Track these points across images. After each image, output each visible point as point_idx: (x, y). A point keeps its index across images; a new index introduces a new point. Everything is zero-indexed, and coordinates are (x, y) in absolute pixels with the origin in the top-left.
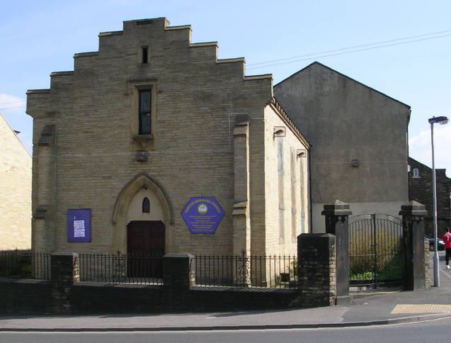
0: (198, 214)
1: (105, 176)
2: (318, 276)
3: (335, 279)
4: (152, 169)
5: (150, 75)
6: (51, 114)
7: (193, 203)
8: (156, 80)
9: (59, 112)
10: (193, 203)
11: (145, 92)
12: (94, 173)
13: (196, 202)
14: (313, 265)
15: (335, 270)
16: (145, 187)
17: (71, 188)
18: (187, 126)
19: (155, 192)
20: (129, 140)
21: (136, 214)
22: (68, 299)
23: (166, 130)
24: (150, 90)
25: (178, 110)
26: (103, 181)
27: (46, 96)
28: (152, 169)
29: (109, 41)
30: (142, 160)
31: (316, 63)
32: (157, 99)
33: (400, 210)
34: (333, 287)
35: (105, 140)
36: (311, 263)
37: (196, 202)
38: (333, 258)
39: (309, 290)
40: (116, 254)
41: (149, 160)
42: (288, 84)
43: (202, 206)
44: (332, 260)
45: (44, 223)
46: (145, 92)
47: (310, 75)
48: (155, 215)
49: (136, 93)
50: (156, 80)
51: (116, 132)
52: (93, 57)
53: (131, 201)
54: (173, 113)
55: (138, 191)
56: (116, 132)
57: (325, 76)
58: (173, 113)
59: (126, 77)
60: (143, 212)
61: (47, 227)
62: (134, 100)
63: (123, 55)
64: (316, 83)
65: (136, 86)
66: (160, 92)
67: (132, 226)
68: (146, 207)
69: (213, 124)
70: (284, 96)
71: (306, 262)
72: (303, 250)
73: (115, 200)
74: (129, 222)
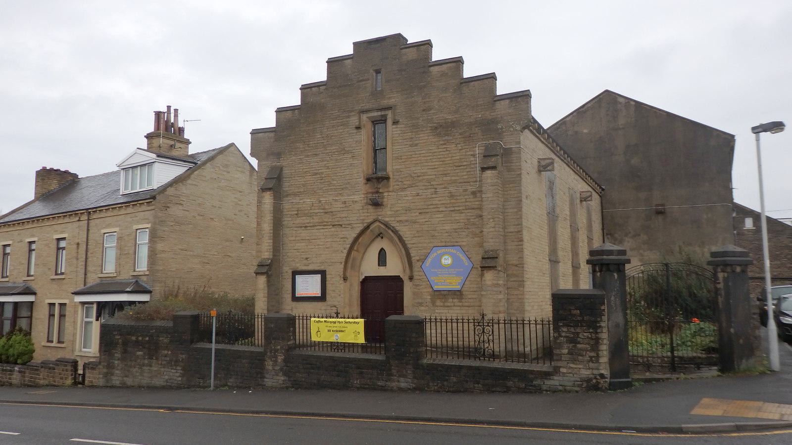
0: (442, 266)
2: (582, 349)
7: (435, 254)
8: (389, 108)
10: (435, 254)
13: (439, 252)
16: (380, 235)
19: (391, 240)
20: (362, 180)
21: (370, 267)
26: (333, 229)
28: (386, 214)
30: (376, 204)
36: (572, 330)
37: (439, 252)
41: (384, 203)
43: (446, 257)
44: (600, 327)
49: (369, 126)
50: (389, 108)
53: (364, 253)
55: (373, 241)
60: (379, 265)
61: (269, 284)
67: (367, 282)
70: (570, 133)
72: (561, 312)
74: (363, 277)
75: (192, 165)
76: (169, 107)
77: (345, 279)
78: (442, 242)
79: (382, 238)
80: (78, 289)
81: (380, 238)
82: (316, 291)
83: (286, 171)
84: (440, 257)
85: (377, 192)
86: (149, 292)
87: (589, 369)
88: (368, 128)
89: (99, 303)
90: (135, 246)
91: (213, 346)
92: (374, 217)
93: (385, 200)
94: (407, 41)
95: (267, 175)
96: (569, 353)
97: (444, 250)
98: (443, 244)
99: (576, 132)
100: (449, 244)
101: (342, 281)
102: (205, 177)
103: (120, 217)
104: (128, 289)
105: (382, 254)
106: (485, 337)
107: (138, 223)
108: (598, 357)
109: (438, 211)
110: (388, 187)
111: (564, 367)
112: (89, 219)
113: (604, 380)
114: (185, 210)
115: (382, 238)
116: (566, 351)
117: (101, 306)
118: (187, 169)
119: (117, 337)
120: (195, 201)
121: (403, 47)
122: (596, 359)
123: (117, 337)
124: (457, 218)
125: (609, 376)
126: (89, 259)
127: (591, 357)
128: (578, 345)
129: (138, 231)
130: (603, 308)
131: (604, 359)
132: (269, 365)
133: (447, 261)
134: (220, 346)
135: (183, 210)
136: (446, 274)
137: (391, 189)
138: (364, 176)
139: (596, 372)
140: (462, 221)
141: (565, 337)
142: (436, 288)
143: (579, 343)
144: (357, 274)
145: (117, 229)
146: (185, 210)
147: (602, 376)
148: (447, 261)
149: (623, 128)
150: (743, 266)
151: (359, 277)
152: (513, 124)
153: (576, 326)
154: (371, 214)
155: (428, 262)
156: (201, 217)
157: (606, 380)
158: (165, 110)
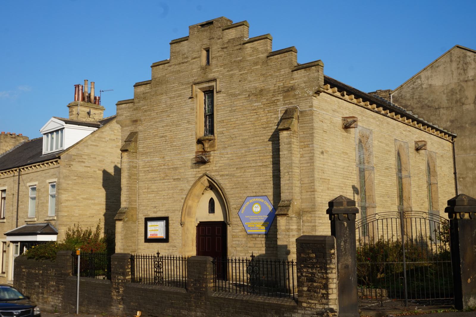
0: (253, 214)
1: (176, 178)
2: (317, 287)
3: (335, 291)
5: (211, 76)
6: (135, 121)
7: (248, 203)
8: (215, 80)
9: (140, 120)
10: (248, 203)
13: (251, 201)
15: (335, 281)
22: (122, 299)
26: (174, 183)
29: (177, 47)
32: (217, 98)
33: (446, 206)
36: (310, 270)
37: (251, 201)
38: (332, 266)
39: (309, 303)
40: (156, 255)
41: (211, 160)
43: (256, 205)
44: (330, 268)
48: (218, 216)
50: (215, 80)
52: (166, 65)
54: (230, 111)
57: (468, 59)
58: (230, 111)
59: (191, 80)
60: (209, 213)
63: (189, 59)
64: (458, 68)
65: (200, 89)
68: (212, 209)
69: (265, 120)
70: (424, 86)
71: (305, 270)
72: (302, 255)
73: (183, 201)
74: (199, 222)
75: (95, 129)
78: (253, 192)
80: (9, 231)
82: (161, 234)
84: (252, 205)
86: (56, 233)
87: (322, 304)
88: (201, 96)
89: (21, 242)
92: (204, 172)
95: (127, 138)
96: (308, 290)
97: (254, 199)
98: (254, 194)
100: (258, 194)
101: (180, 226)
102: (105, 138)
103: (39, 173)
105: (212, 202)
106: (254, 276)
107: (50, 177)
108: (328, 294)
109: (250, 167)
111: (304, 302)
112: (19, 175)
113: (333, 314)
114: (87, 167)
116: (305, 289)
117: (23, 243)
118: (91, 132)
119: (24, 270)
120: (95, 158)
122: (326, 296)
123: (24, 270)
124: (264, 172)
125: (338, 311)
126: (20, 207)
127: (323, 294)
128: (314, 284)
130: (332, 251)
131: (334, 295)
133: (257, 208)
135: (85, 166)
136: (256, 220)
137: (216, 148)
139: (326, 307)
140: (268, 174)
141: (306, 276)
142: (249, 231)
143: (315, 282)
146: (87, 167)
147: (332, 310)
148: (257, 208)
149: (473, 80)
152: (307, 90)
153: (312, 268)
157: (336, 314)
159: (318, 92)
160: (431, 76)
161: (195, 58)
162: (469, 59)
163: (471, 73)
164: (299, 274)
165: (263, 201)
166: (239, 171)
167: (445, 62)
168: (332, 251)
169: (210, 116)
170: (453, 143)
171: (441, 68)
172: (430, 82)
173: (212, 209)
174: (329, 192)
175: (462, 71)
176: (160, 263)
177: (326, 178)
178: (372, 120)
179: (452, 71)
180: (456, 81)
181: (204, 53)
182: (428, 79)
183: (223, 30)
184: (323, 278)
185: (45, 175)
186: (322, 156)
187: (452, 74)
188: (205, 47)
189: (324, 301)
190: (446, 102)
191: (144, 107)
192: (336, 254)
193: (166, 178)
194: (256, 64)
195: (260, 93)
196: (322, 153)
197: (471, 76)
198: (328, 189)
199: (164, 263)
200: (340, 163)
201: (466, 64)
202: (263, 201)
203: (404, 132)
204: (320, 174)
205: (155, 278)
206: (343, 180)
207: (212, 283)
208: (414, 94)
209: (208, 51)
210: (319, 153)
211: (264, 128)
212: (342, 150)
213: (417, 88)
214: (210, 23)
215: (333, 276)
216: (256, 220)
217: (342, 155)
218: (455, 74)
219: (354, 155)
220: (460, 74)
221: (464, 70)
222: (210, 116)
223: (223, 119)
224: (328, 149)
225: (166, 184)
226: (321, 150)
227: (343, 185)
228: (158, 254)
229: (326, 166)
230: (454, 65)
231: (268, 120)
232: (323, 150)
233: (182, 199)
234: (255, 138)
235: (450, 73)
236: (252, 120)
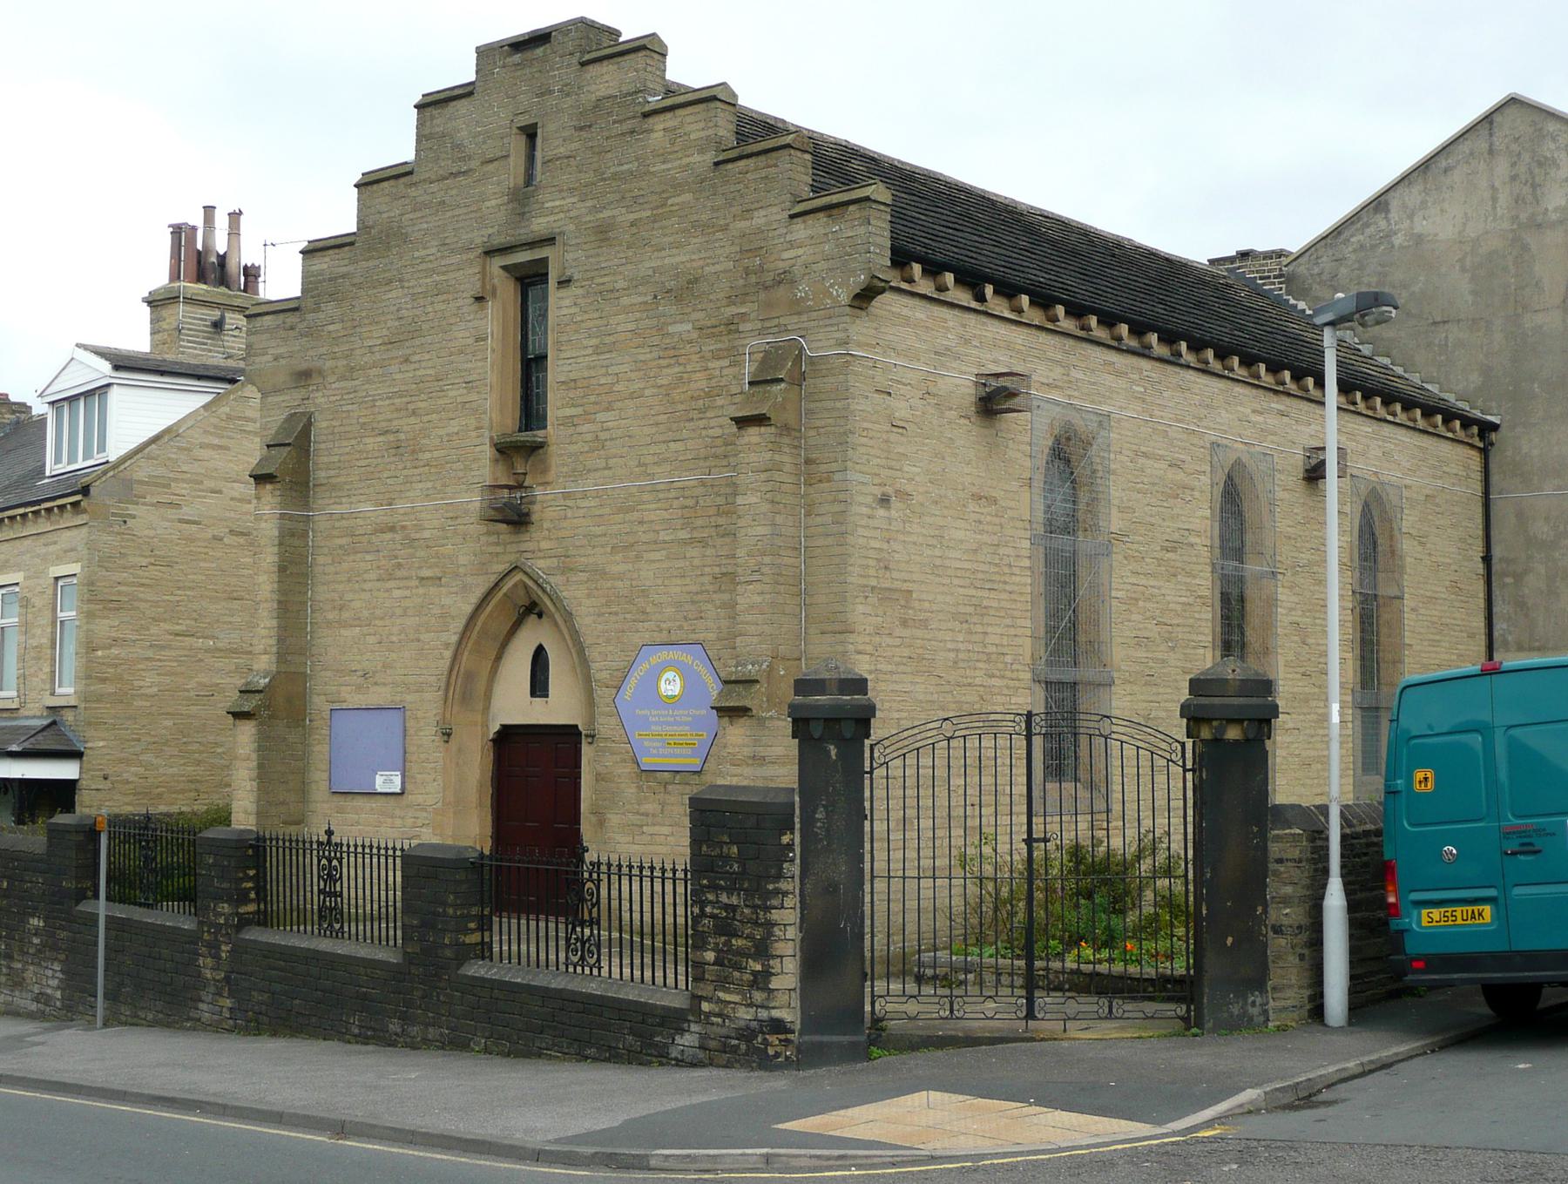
1: (426, 573)
2: (741, 953)
4: (540, 552)
5: (539, 225)
6: (304, 376)
8: (550, 241)
9: (320, 372)
11: (530, 279)
12: (399, 566)
13: (654, 660)
14: (727, 907)
15: (792, 932)
16: (532, 609)
17: (346, 615)
18: (632, 397)
20: (488, 452)
21: (514, 704)
22: (227, 979)
23: (580, 410)
24: (544, 278)
25: (608, 340)
26: (421, 591)
27: (291, 319)
28: (540, 552)
29: (440, 117)
30: (514, 517)
31: (1513, 102)
32: (559, 304)
34: (782, 998)
35: (428, 455)
36: (724, 898)
37: (654, 660)
38: (783, 885)
39: (719, 1001)
40: (324, 838)
41: (534, 518)
42: (1413, 195)
43: (670, 675)
44: (777, 892)
45: (254, 731)
46: (530, 279)
47: (1491, 152)
48: (557, 710)
50: (550, 241)
51: (454, 427)
53: (499, 658)
54: (597, 351)
56: (454, 427)
58: (597, 351)
59: (480, 237)
60: (533, 694)
61: (265, 746)
62: (495, 323)
63: (474, 164)
64: (1514, 178)
65: (505, 268)
66: (564, 283)
67: (509, 740)
68: (539, 686)
69: (703, 384)
70: (1398, 240)
71: (711, 897)
73: (448, 654)
74: (497, 728)
75: (221, 387)
76: (209, 211)
77: (447, 735)
79: (540, 615)
81: (533, 617)
83: (321, 424)
85: (520, 486)
86: (75, 755)
87: (750, 1005)
88: (508, 291)
90: (54, 623)
91: (102, 908)
92: (512, 558)
93: (536, 508)
94: (618, 34)
95: (277, 433)
96: (718, 962)
98: (664, 637)
99: (1419, 239)
100: (673, 638)
103: (27, 542)
104: (14, 748)
105: (539, 659)
107: (59, 560)
108: (767, 974)
109: (655, 542)
110: (545, 471)
113: (782, 1037)
114: (188, 522)
115: (540, 615)
116: (710, 956)
118: (209, 398)
120: (220, 492)
121: (587, 57)
122: (761, 980)
124: (696, 562)
125: (798, 1027)
127: (755, 973)
129: (60, 583)
130: (785, 839)
131: (787, 974)
132: (205, 963)
133: (671, 685)
134: (122, 911)
135: (180, 521)
136: (668, 723)
137: (551, 476)
138: (491, 438)
139: (763, 1014)
141: (713, 916)
142: (647, 762)
143: (736, 936)
144: (479, 718)
145: (17, 577)
146: (188, 522)
147: (778, 1026)
148: (671, 685)
150: (1215, 723)
151: (485, 725)
152: (832, 286)
153: (730, 891)
154: (503, 550)
155: (628, 691)
156: (242, 540)
157: (790, 1036)
158: (197, 220)
159: (865, 296)
160: (1424, 204)
161: (491, 161)
162: (1552, 146)
163: (1554, 200)
164: (696, 910)
165: (689, 660)
166: (619, 557)
167: (1472, 154)
168: (785, 839)
169: (532, 366)
170: (1485, 452)
171: (1457, 176)
172: (1421, 226)
173: (539, 686)
174: (906, 633)
175: (1527, 190)
176: (335, 863)
177: (897, 585)
178: (1109, 380)
179: (1493, 187)
180: (1506, 225)
181: (518, 144)
182: (1411, 217)
183: (583, 64)
184: (756, 923)
185: (44, 550)
186: (881, 512)
187: (1494, 199)
188: (524, 120)
189: (758, 996)
190: (1470, 298)
191: (331, 328)
192: (798, 850)
193: (399, 573)
194: (678, 187)
195: (686, 289)
196: (884, 501)
197: (1556, 210)
198: (904, 623)
199: (345, 861)
200: (960, 535)
201: (1540, 164)
202: (689, 660)
203: (1255, 418)
204: (872, 572)
205: (320, 910)
206: (972, 592)
207: (473, 931)
208: (1361, 268)
209: (530, 133)
210: (869, 499)
211: (700, 411)
212: (975, 490)
213: (1373, 247)
214: (539, 39)
215: (787, 916)
216: (668, 723)
217: (972, 506)
218: (1504, 199)
219: (1023, 503)
220: (1518, 200)
221: (1534, 186)
222: (532, 366)
223: (573, 376)
224: (909, 488)
225: (397, 593)
226: (878, 491)
227: (970, 610)
228: (329, 833)
229: (895, 546)
230: (1502, 167)
231: (713, 383)
232: (889, 490)
233: (447, 645)
234: (672, 445)
235: (1487, 195)
236: (665, 382)
